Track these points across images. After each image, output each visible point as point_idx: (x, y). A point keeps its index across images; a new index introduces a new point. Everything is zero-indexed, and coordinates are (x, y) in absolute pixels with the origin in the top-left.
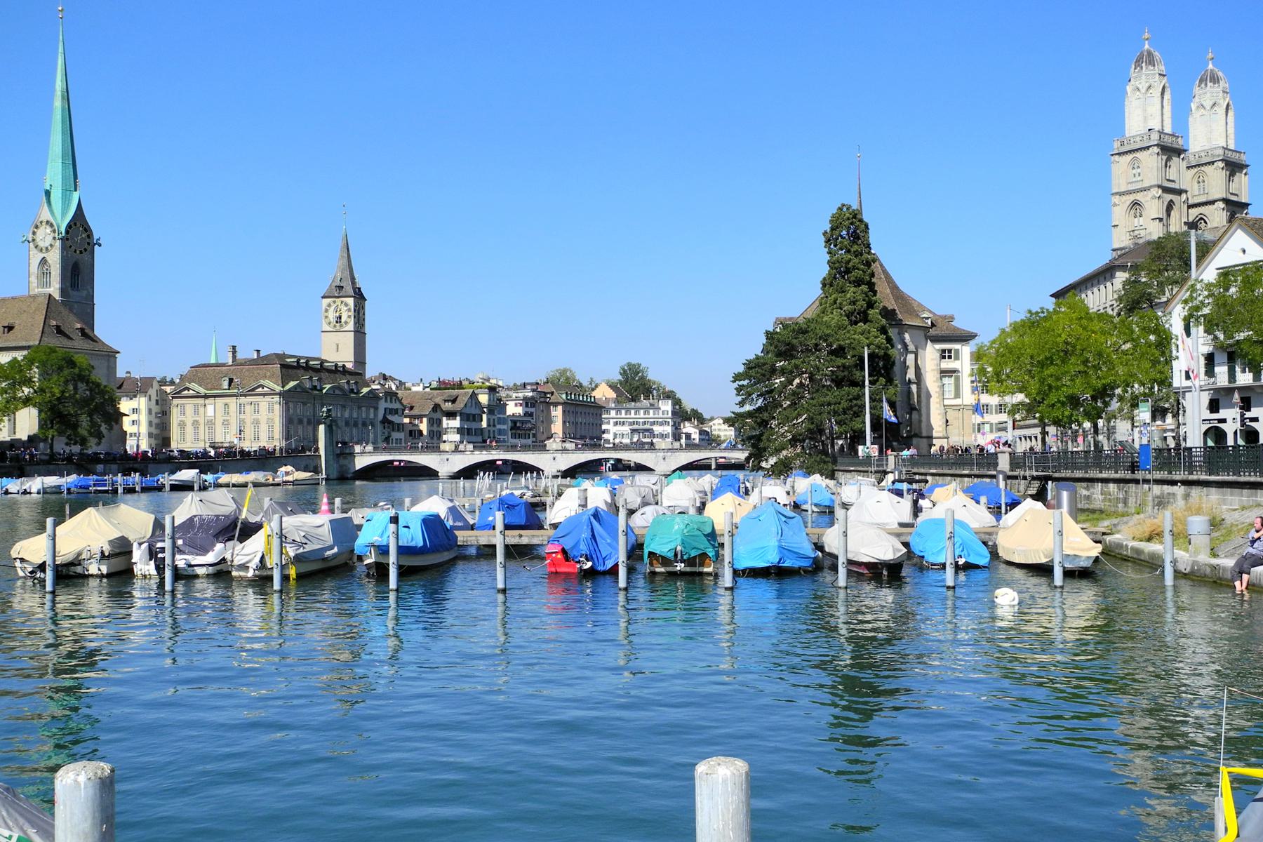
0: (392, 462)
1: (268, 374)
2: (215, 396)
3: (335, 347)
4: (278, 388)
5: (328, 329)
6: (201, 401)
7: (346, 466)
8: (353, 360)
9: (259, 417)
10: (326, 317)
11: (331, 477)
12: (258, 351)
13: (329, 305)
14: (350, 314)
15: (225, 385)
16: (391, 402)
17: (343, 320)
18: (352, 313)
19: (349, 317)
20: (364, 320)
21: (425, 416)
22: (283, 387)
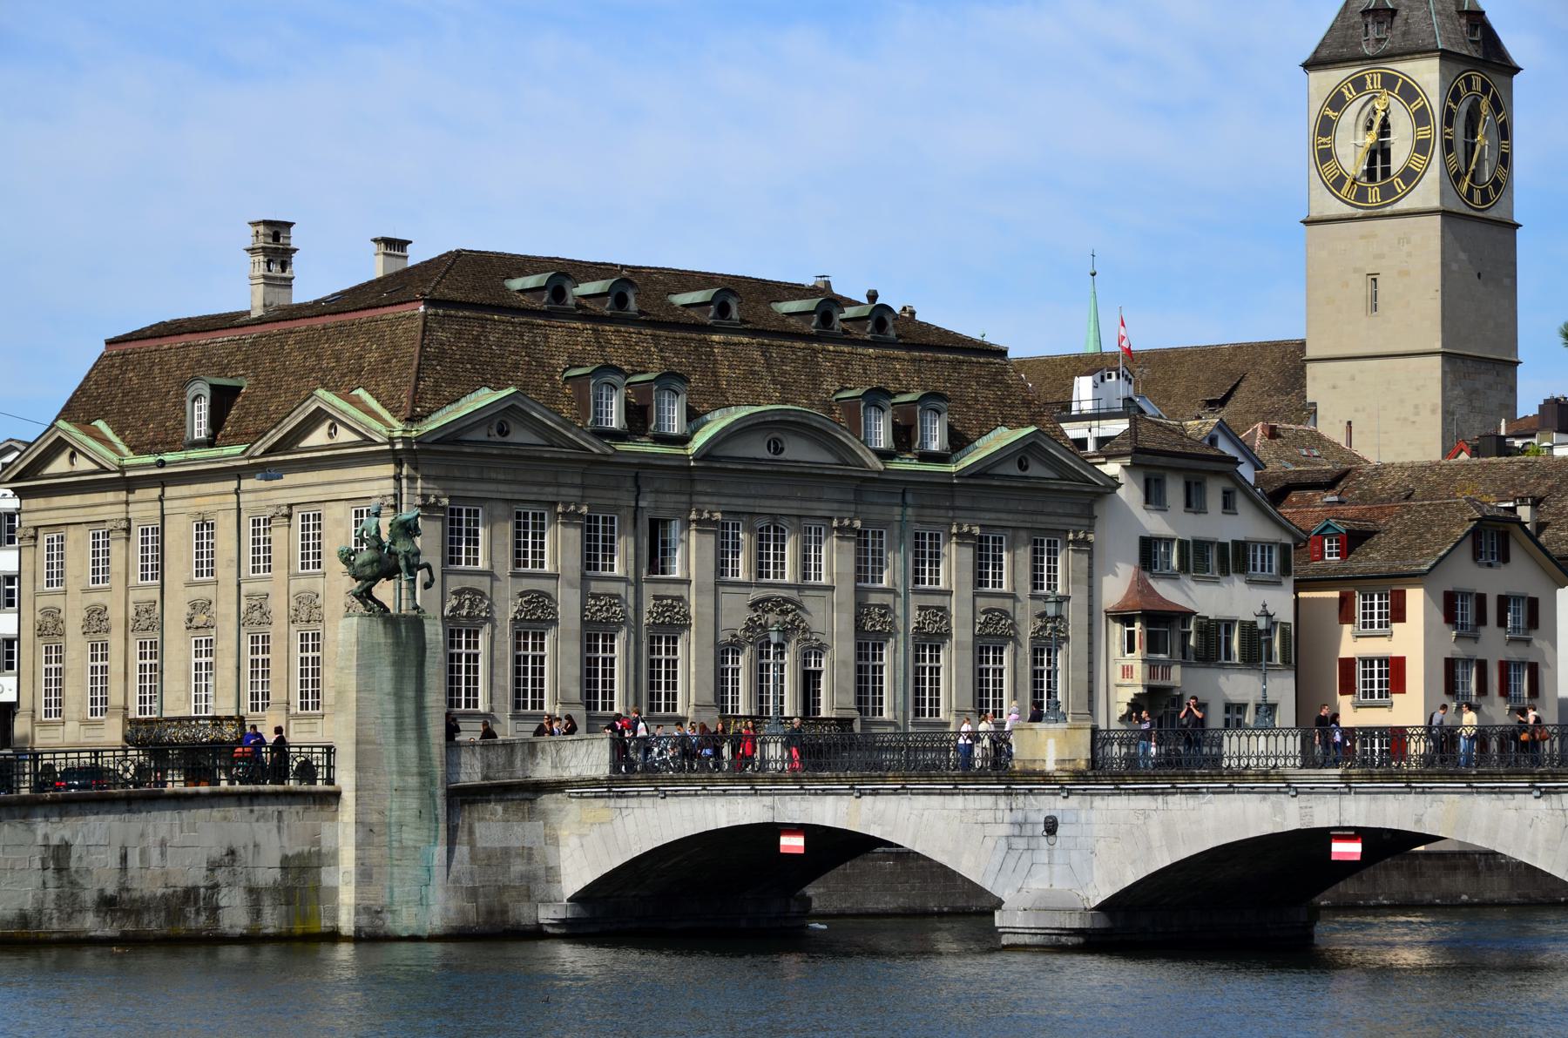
0: (774, 830)
1: (373, 356)
2: (163, 481)
3: (1361, 288)
4: (387, 427)
5: (1337, 208)
6: (107, 506)
7: (528, 854)
8: (1437, 345)
9: (319, 585)
10: (1325, 155)
11: (405, 920)
12: (395, 245)
13: (1337, 102)
14: (1424, 133)
15: (199, 423)
16: (1194, 502)
17: (1396, 165)
18: (1434, 131)
19: (1422, 147)
20: (1505, 160)
21: (1415, 578)
22: (412, 419)
